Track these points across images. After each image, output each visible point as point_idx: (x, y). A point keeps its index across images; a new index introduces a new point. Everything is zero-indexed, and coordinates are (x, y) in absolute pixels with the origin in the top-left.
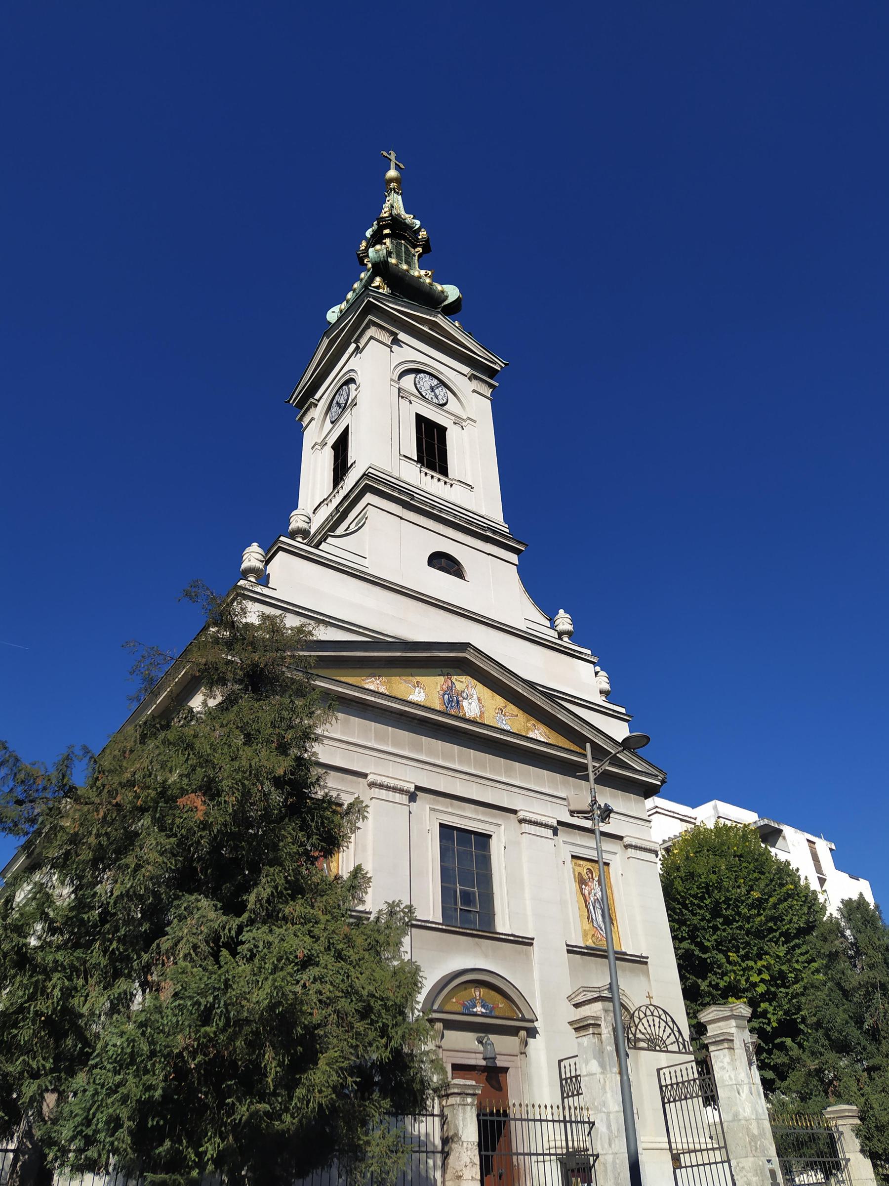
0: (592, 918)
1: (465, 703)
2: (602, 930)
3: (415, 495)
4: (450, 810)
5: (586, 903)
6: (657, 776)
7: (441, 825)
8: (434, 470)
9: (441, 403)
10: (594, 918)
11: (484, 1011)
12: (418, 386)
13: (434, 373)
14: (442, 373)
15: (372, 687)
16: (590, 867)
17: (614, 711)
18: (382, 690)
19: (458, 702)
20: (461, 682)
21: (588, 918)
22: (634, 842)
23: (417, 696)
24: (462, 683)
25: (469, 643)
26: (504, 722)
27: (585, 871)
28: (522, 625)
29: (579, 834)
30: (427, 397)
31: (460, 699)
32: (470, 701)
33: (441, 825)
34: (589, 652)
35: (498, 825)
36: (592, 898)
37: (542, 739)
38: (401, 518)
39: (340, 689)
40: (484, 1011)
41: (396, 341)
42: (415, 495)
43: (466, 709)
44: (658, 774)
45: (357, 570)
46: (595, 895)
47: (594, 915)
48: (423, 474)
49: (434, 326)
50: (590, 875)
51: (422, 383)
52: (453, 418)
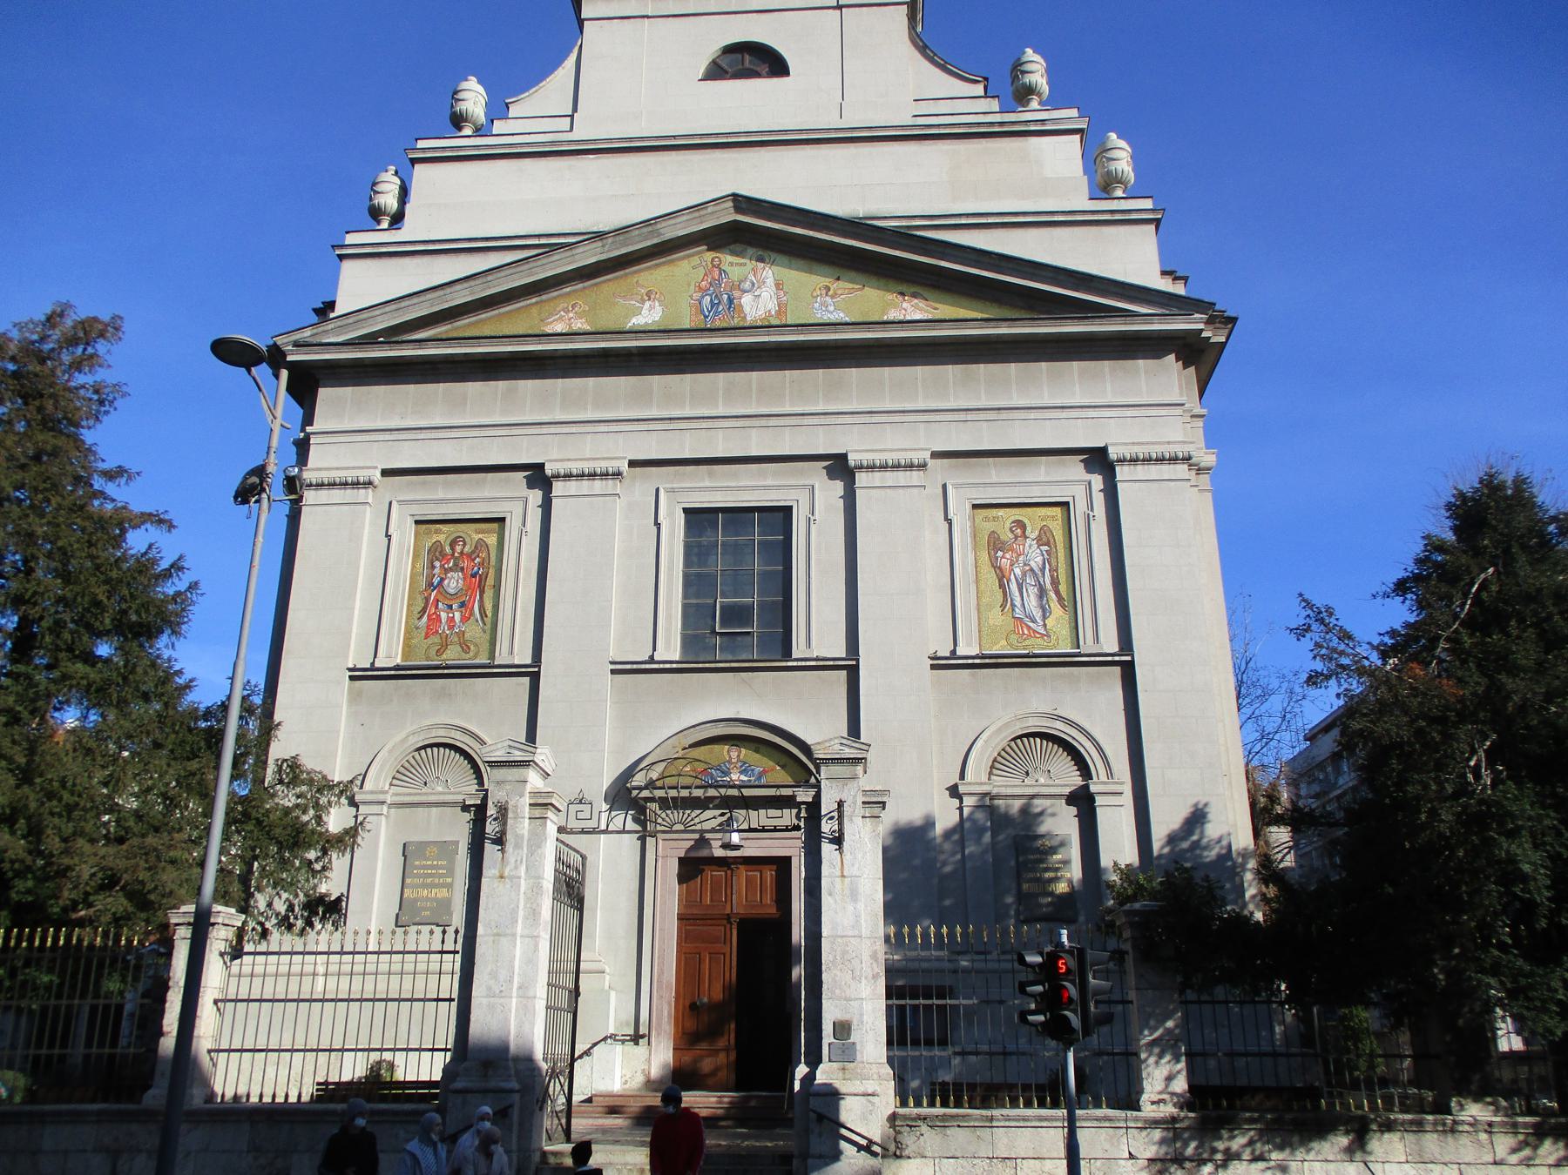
0: (1013, 605)
1: (746, 300)
2: (1034, 621)
4: (707, 484)
7: (685, 510)
10: (1018, 602)
11: (743, 778)
15: (559, 328)
16: (1017, 518)
17: (1112, 212)
18: (580, 325)
19: (731, 301)
21: (1003, 606)
23: (649, 315)
27: (1008, 525)
28: (901, 115)
29: (995, 465)
31: (736, 294)
33: (685, 510)
34: (1074, 113)
37: (918, 316)
38: (648, 17)
40: (746, 779)
43: (747, 309)
45: (553, 143)
46: (1025, 565)
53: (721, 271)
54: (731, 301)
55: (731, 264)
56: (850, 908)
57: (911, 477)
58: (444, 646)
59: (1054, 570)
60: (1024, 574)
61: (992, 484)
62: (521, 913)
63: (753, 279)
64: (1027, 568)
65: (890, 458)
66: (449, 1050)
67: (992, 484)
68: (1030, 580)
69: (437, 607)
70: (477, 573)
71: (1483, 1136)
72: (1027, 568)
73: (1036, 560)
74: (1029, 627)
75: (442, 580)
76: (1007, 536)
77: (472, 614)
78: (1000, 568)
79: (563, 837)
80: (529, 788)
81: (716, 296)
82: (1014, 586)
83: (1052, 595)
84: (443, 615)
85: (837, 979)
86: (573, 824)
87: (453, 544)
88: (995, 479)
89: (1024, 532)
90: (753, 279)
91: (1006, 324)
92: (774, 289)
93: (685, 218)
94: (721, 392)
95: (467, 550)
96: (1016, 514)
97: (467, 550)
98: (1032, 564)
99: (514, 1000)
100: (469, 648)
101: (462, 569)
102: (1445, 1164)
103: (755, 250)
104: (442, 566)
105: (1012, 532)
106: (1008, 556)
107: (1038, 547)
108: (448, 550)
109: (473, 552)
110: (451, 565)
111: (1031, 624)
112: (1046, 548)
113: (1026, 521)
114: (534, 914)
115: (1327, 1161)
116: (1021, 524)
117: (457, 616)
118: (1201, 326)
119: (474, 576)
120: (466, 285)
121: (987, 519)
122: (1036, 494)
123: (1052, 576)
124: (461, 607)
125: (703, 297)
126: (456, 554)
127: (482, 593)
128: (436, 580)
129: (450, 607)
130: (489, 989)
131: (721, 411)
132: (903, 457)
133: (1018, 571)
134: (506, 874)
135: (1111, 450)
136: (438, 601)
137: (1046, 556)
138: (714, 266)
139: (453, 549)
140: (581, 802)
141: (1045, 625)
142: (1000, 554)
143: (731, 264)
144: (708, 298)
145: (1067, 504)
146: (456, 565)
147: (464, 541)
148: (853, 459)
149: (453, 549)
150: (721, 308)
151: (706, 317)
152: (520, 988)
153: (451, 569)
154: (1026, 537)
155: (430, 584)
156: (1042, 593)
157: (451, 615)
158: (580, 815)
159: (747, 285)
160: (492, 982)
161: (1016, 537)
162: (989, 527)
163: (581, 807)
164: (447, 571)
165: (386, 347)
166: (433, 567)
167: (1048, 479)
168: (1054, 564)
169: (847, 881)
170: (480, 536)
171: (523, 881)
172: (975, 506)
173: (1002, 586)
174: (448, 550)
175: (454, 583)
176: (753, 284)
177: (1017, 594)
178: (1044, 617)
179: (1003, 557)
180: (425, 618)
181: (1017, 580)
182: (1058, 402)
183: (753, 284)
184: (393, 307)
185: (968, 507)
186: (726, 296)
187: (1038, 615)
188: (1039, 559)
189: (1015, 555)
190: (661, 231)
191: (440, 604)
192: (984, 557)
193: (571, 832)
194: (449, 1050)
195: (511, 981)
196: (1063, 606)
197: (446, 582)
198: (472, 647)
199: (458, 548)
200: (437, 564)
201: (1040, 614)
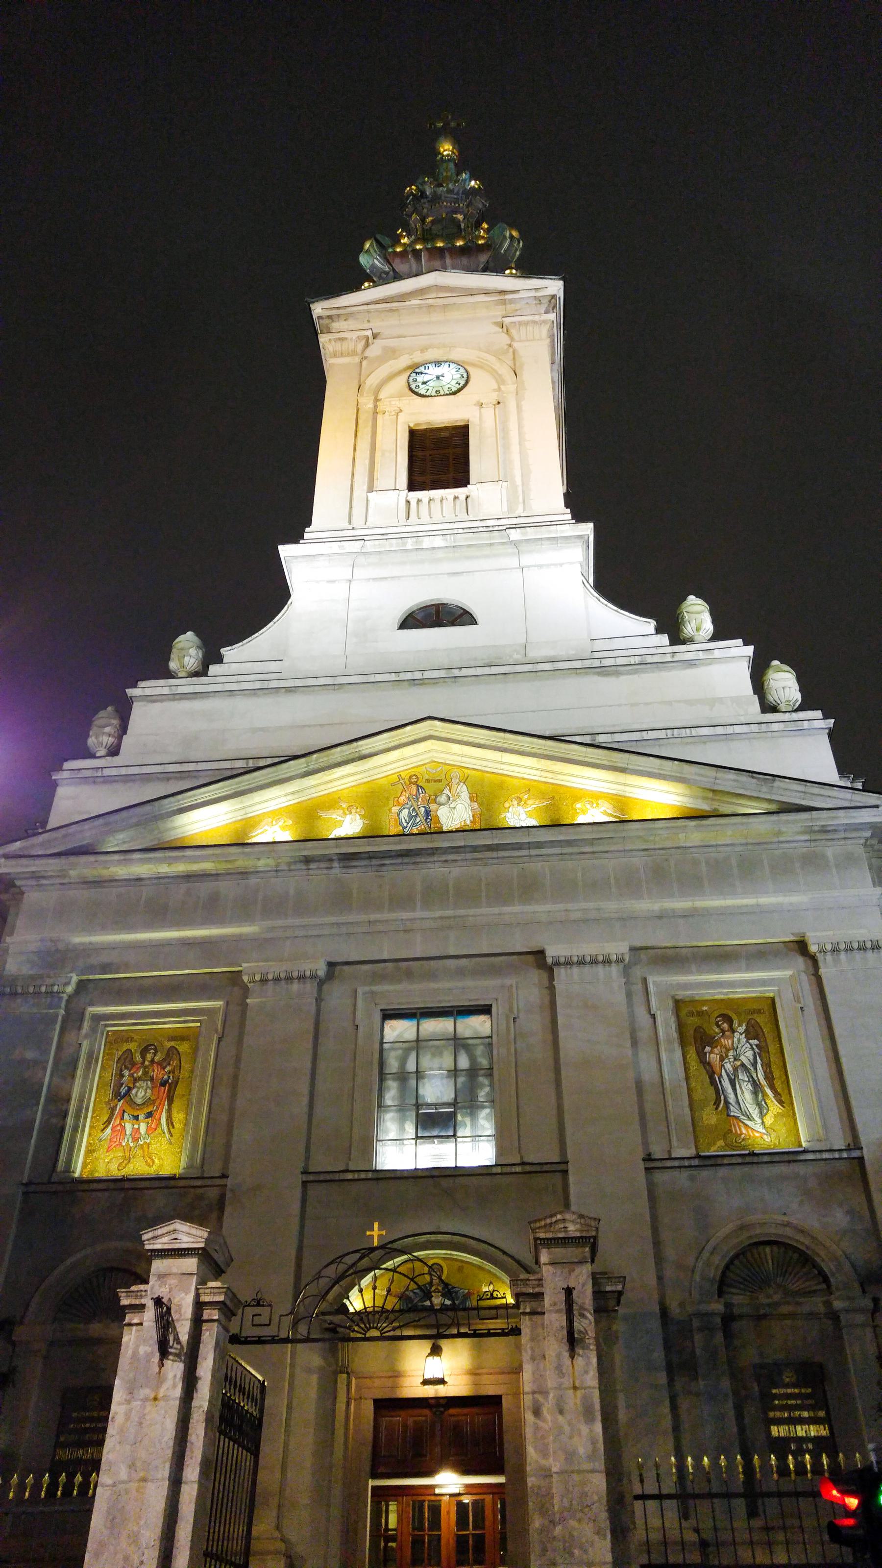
0: (727, 1103)
9: (454, 389)
12: (413, 387)
19: (428, 813)
21: (717, 1103)
30: (428, 394)
31: (433, 807)
32: (452, 806)
36: (728, 1066)
46: (735, 1059)
50: (726, 1026)
53: (418, 786)
54: (428, 813)
56: (584, 1429)
60: (735, 1069)
63: (449, 793)
64: (738, 1063)
68: (743, 1076)
69: (122, 1118)
70: (166, 1082)
72: (738, 1063)
73: (747, 1056)
77: (159, 1124)
78: (709, 1064)
81: (414, 809)
85: (575, 1534)
86: (250, 1332)
87: (144, 1052)
90: (449, 793)
92: (468, 801)
95: (157, 1059)
97: (157, 1059)
98: (742, 1058)
100: (153, 1163)
101: (152, 1079)
104: (131, 1075)
105: (718, 1026)
106: (716, 1051)
107: (747, 1041)
108: (138, 1058)
109: (164, 1060)
110: (140, 1074)
111: (748, 1122)
112: (756, 1042)
113: (734, 1017)
117: (143, 1128)
119: (163, 1084)
124: (147, 1117)
125: (401, 810)
126: (147, 1063)
128: (123, 1090)
129: (136, 1118)
133: (728, 1066)
134: (161, 1395)
136: (124, 1111)
137: (757, 1050)
138: (411, 783)
139: (143, 1057)
140: (258, 1305)
146: (145, 1073)
148: (551, 952)
149: (143, 1057)
150: (418, 820)
153: (140, 1079)
157: (136, 1126)
158: (257, 1320)
159: (443, 799)
163: (258, 1310)
164: (135, 1080)
166: (122, 1076)
169: (579, 1393)
170: (172, 1044)
173: (713, 1082)
174: (138, 1058)
176: (449, 797)
177: (729, 1090)
179: (711, 1052)
180: (109, 1130)
181: (728, 1075)
183: (449, 797)
186: (423, 809)
188: (750, 1054)
189: (724, 1050)
191: (126, 1115)
192: (692, 1054)
197: (134, 1091)
198: (156, 1160)
199: (149, 1057)
200: (126, 1073)
201: (757, 1111)
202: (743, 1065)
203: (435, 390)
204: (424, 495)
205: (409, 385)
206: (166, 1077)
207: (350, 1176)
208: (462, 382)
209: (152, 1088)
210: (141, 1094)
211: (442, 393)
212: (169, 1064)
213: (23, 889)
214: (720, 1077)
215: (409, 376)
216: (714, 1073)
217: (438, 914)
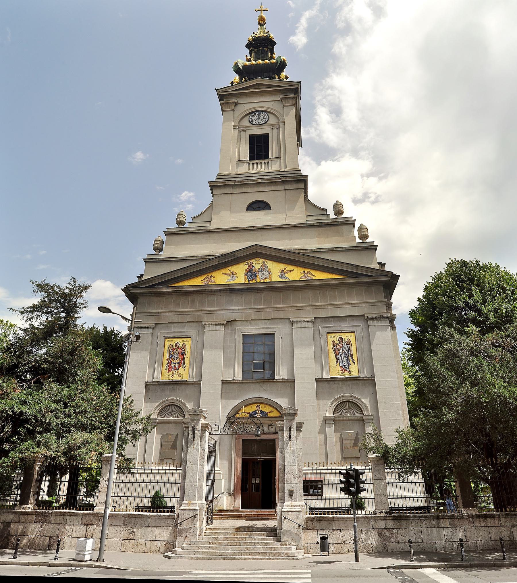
2: (346, 367)
3: (236, 179)
4: (250, 327)
5: (336, 355)
6: (387, 275)
8: (261, 159)
9: (264, 122)
10: (341, 362)
12: (251, 121)
13: (260, 109)
14: (264, 107)
19: (255, 274)
20: (258, 264)
22: (370, 316)
24: (257, 264)
25: (256, 244)
26: (284, 276)
35: (278, 328)
39: (184, 289)
41: (236, 104)
42: (236, 179)
44: (387, 274)
45: (205, 230)
47: (341, 361)
48: (251, 166)
49: (258, 85)
51: (253, 118)
52: (271, 127)
55: (256, 264)
57: (309, 324)
58: (173, 375)
59: (351, 352)
60: (343, 353)
61: (333, 327)
62: (199, 458)
65: (302, 319)
66: (179, 498)
67: (333, 327)
71: (471, 519)
73: (346, 349)
74: (344, 369)
75: (173, 355)
76: (337, 342)
78: (335, 351)
79: (210, 436)
80: (201, 422)
82: (340, 357)
83: (351, 360)
84: (173, 366)
86: (213, 432)
87: (176, 344)
88: (333, 325)
89: (342, 341)
91: (334, 280)
93: (242, 251)
94: (253, 301)
96: (339, 335)
98: (345, 350)
99: (197, 483)
102: (461, 527)
103: (262, 260)
105: (339, 341)
109: (182, 347)
111: (345, 368)
112: (349, 345)
113: (343, 338)
114: (203, 458)
115: (428, 528)
116: (341, 338)
118: (390, 279)
120: (180, 271)
121: (331, 337)
122: (345, 329)
123: (351, 354)
127: (184, 359)
128: (171, 356)
130: (190, 480)
131: (253, 307)
132: (306, 319)
133: (341, 352)
135: (366, 316)
138: (250, 264)
140: (215, 426)
141: (349, 368)
142: (335, 347)
143: (256, 264)
144: (249, 274)
145: (355, 332)
147: (179, 344)
151: (248, 279)
152: (199, 480)
154: (343, 342)
155: (169, 357)
156: (348, 359)
160: (191, 478)
161: (340, 342)
162: (332, 339)
165: (158, 288)
167: (348, 325)
168: (351, 350)
171: (199, 449)
172: (328, 333)
173: (336, 357)
175: (176, 356)
177: (341, 359)
178: (349, 366)
182: (350, 302)
184: (160, 277)
185: (326, 333)
187: (347, 366)
188: (347, 349)
189: (340, 347)
190: (236, 255)
193: (213, 434)
194: (179, 498)
195: (196, 478)
196: (354, 363)
197: (174, 356)
199: (177, 346)
200: (171, 351)
202: (345, 352)
203: (258, 122)
204: (255, 162)
205: (249, 121)
206: (182, 352)
207: (235, 381)
208: (267, 120)
209: (179, 355)
210: (176, 357)
211: (260, 124)
212: (183, 348)
213: (138, 296)
214: (338, 355)
215: (250, 117)
216: (336, 354)
217: (259, 307)
